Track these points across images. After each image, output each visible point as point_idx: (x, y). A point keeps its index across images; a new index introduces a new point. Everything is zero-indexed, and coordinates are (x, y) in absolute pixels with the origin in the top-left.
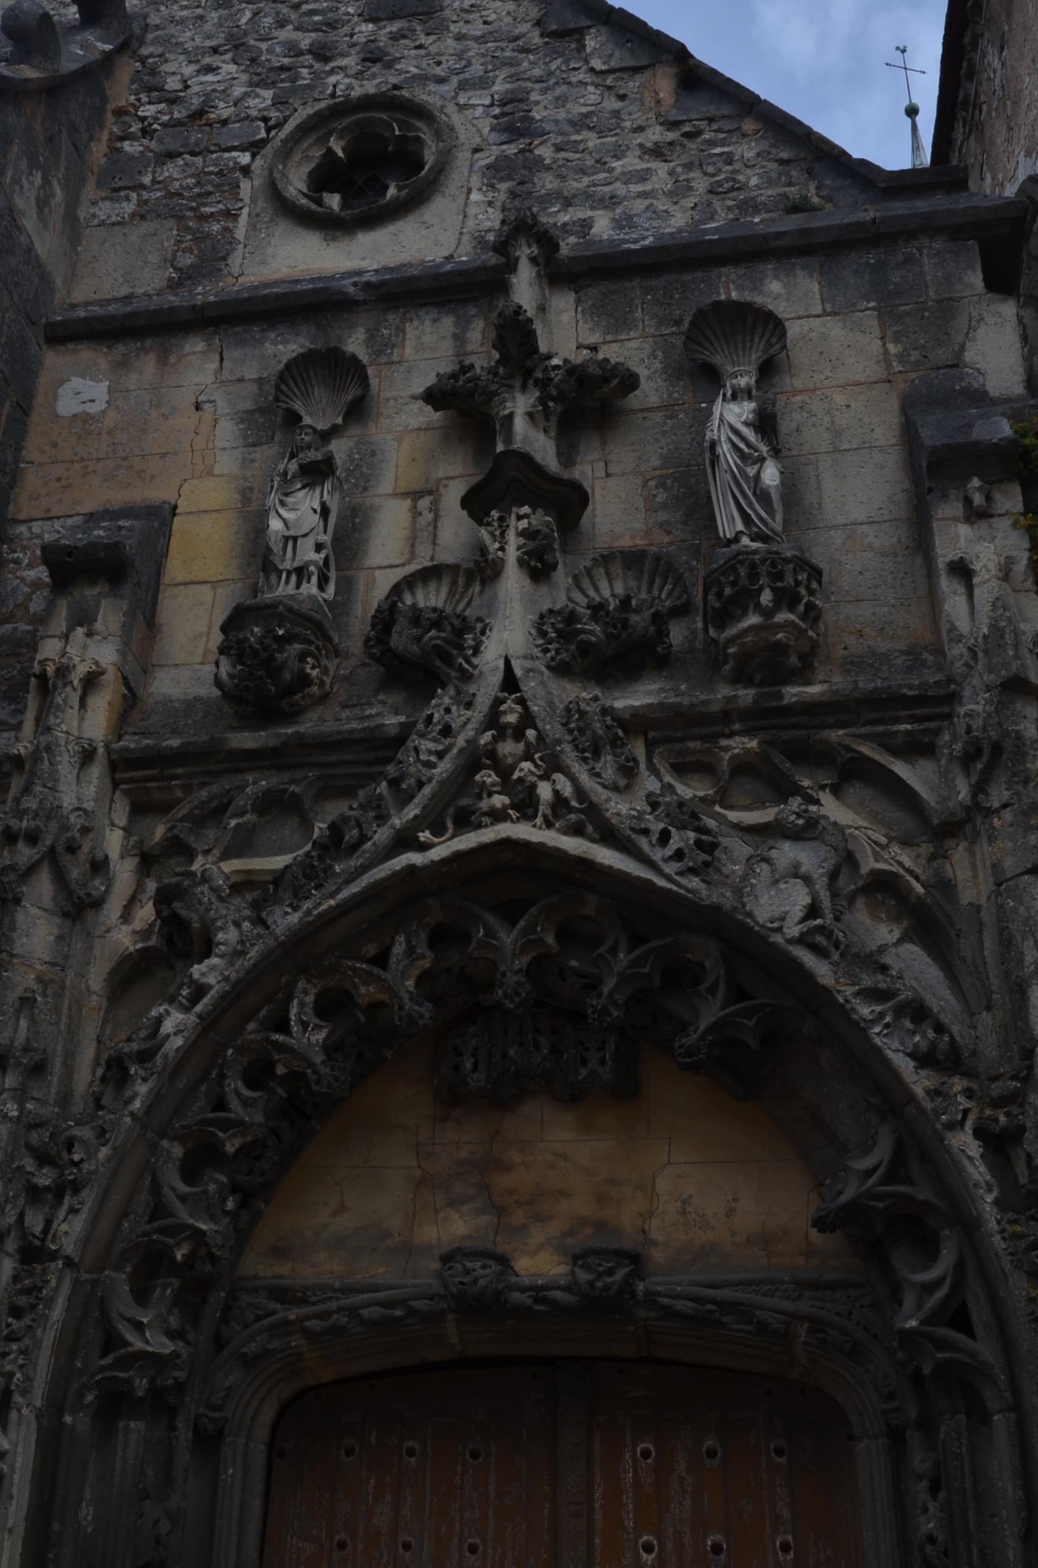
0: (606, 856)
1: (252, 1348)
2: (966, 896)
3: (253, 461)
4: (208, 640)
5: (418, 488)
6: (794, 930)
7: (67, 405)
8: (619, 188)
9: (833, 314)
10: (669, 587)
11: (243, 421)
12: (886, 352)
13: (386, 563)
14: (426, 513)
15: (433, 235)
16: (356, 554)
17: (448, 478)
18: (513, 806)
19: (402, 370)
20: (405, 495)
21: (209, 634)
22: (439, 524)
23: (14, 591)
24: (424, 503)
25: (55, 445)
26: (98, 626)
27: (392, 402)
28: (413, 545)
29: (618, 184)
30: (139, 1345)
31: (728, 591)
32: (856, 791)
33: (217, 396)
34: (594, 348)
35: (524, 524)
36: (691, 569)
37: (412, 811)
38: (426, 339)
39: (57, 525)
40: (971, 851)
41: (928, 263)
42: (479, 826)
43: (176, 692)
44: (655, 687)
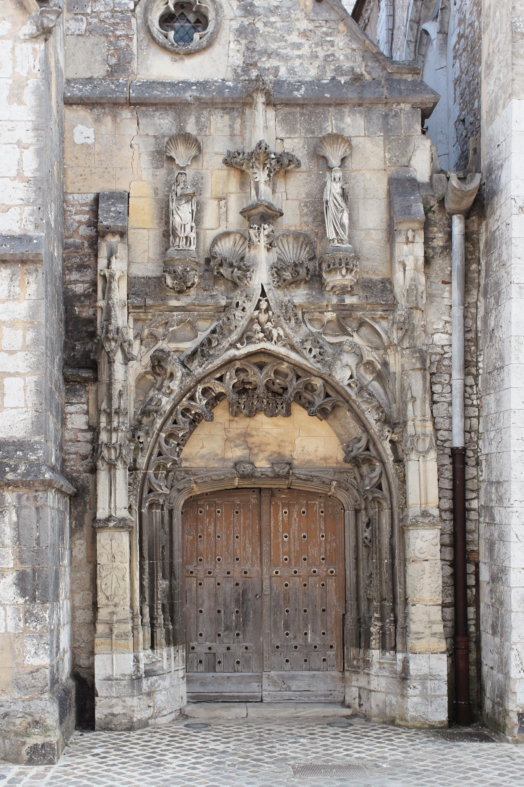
0: (294, 356)
1: (181, 487)
2: (392, 369)
5: (220, 196)
6: (346, 382)
7: (78, 139)
8: (289, 51)
9: (368, 136)
10: (308, 249)
12: (385, 157)
13: (210, 227)
15: (215, 64)
18: (265, 336)
23: (72, 224)
24: (222, 203)
25: (77, 158)
26: (118, 255)
29: (289, 49)
30: (161, 491)
31: (331, 266)
34: (282, 140)
35: (266, 232)
36: (315, 242)
37: (234, 337)
38: (219, 125)
39: (84, 196)
40: (395, 354)
42: (255, 343)
43: (140, 274)
44: (305, 292)
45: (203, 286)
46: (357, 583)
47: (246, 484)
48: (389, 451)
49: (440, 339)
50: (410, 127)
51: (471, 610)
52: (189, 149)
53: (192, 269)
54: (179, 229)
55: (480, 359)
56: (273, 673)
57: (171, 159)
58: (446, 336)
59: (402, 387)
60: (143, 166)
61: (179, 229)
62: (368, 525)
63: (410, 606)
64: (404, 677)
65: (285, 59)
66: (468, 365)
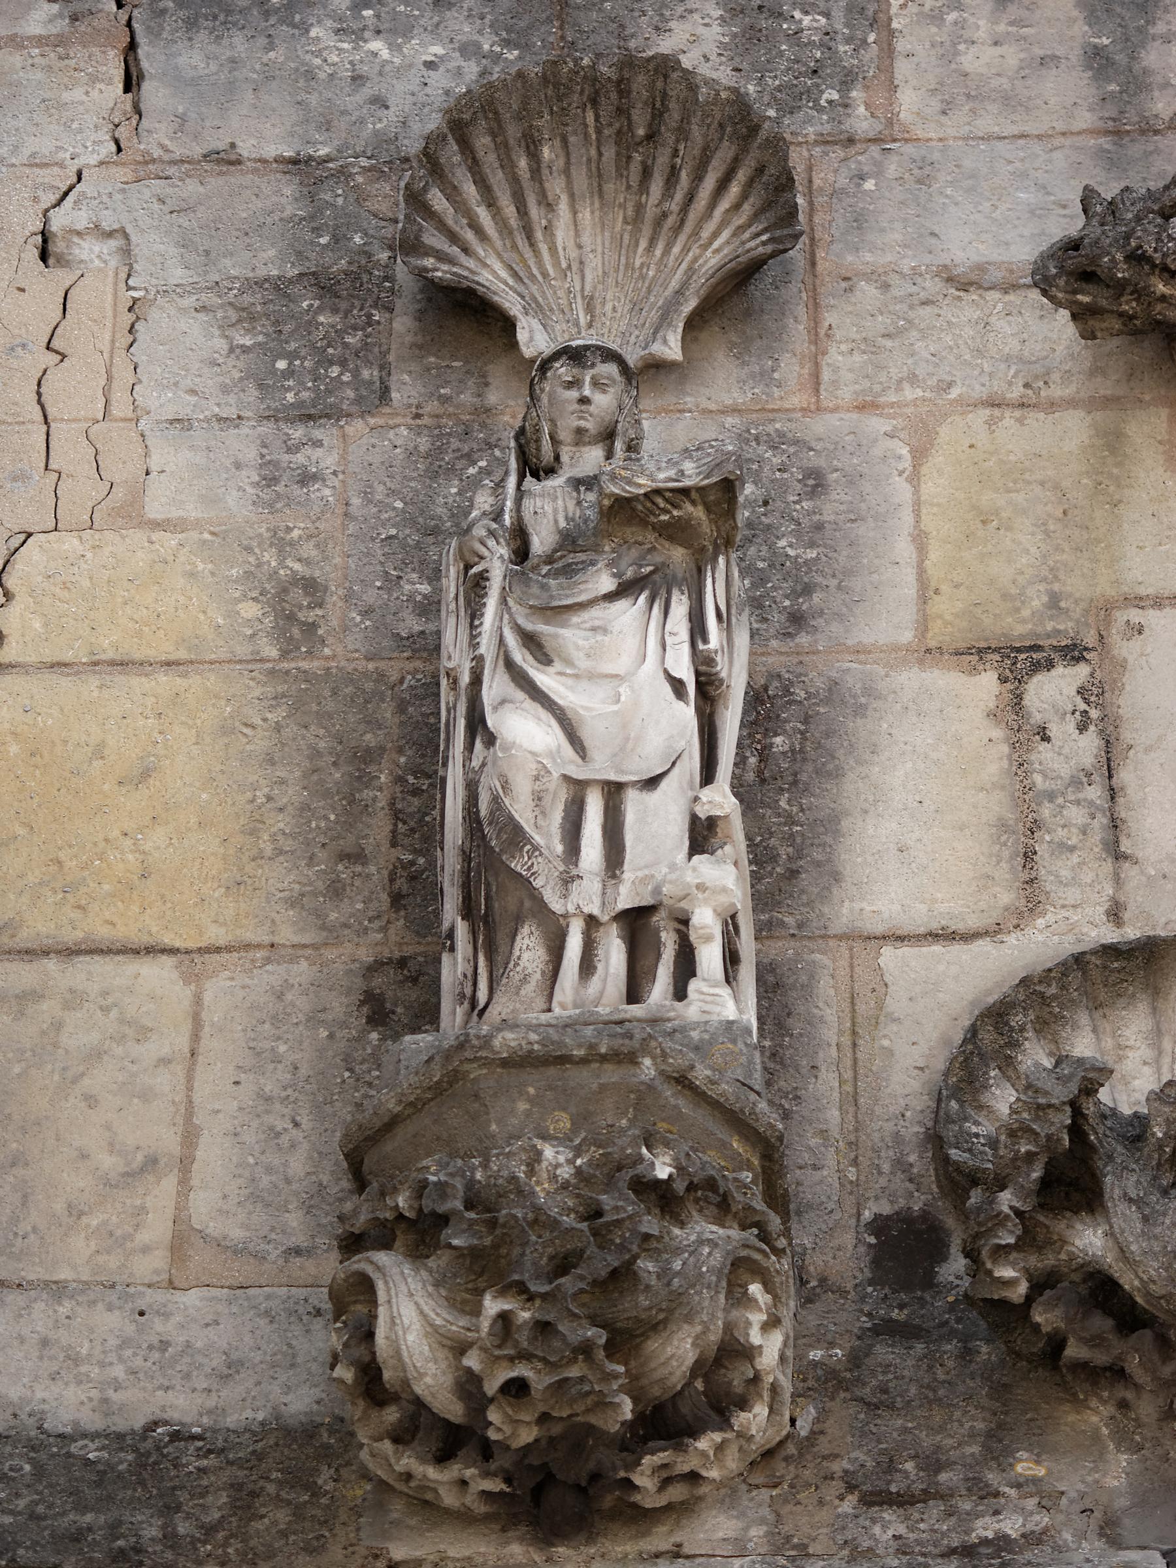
3: (306, 478)
4: (184, 1182)
5: (1019, 629)
11: (247, 317)
13: (919, 918)
14: (1063, 730)
16: (793, 874)
17: (1138, 602)
19: (892, 169)
20: (976, 653)
21: (185, 1163)
22: (1125, 776)
24: (1056, 689)
27: (867, 291)
28: (1029, 856)
33: (139, 208)
38: (976, 60)
45: (856, 1457)
52: (666, 227)
53: (712, 1195)
54: (547, 835)
57: (468, 318)
60: (160, 402)
61: (547, 835)
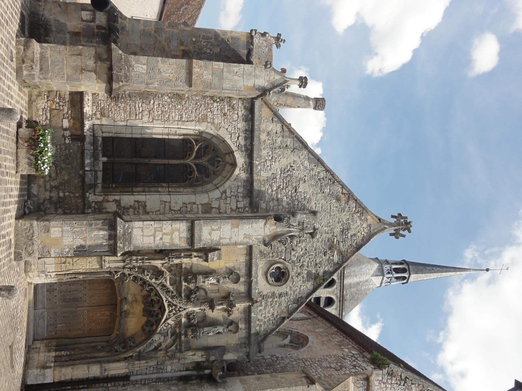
0: (163, 320)
2: (159, 353)
8: (267, 309)
32: (172, 342)
41: (245, 349)
46: (81, 343)
47: (118, 302)
48: (129, 355)
49: (169, 368)
50: (242, 352)
51: (70, 387)
55: (162, 383)
56: (46, 313)
57: (232, 274)
58: (170, 370)
59: (152, 358)
62: (103, 347)
63: (71, 367)
64: (44, 367)
65: (265, 309)
66: (159, 380)
